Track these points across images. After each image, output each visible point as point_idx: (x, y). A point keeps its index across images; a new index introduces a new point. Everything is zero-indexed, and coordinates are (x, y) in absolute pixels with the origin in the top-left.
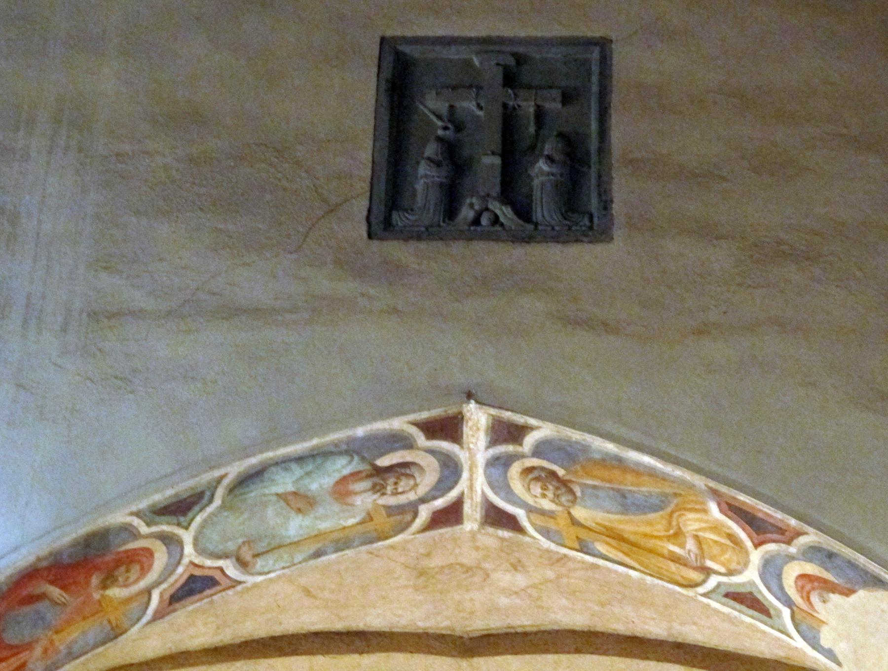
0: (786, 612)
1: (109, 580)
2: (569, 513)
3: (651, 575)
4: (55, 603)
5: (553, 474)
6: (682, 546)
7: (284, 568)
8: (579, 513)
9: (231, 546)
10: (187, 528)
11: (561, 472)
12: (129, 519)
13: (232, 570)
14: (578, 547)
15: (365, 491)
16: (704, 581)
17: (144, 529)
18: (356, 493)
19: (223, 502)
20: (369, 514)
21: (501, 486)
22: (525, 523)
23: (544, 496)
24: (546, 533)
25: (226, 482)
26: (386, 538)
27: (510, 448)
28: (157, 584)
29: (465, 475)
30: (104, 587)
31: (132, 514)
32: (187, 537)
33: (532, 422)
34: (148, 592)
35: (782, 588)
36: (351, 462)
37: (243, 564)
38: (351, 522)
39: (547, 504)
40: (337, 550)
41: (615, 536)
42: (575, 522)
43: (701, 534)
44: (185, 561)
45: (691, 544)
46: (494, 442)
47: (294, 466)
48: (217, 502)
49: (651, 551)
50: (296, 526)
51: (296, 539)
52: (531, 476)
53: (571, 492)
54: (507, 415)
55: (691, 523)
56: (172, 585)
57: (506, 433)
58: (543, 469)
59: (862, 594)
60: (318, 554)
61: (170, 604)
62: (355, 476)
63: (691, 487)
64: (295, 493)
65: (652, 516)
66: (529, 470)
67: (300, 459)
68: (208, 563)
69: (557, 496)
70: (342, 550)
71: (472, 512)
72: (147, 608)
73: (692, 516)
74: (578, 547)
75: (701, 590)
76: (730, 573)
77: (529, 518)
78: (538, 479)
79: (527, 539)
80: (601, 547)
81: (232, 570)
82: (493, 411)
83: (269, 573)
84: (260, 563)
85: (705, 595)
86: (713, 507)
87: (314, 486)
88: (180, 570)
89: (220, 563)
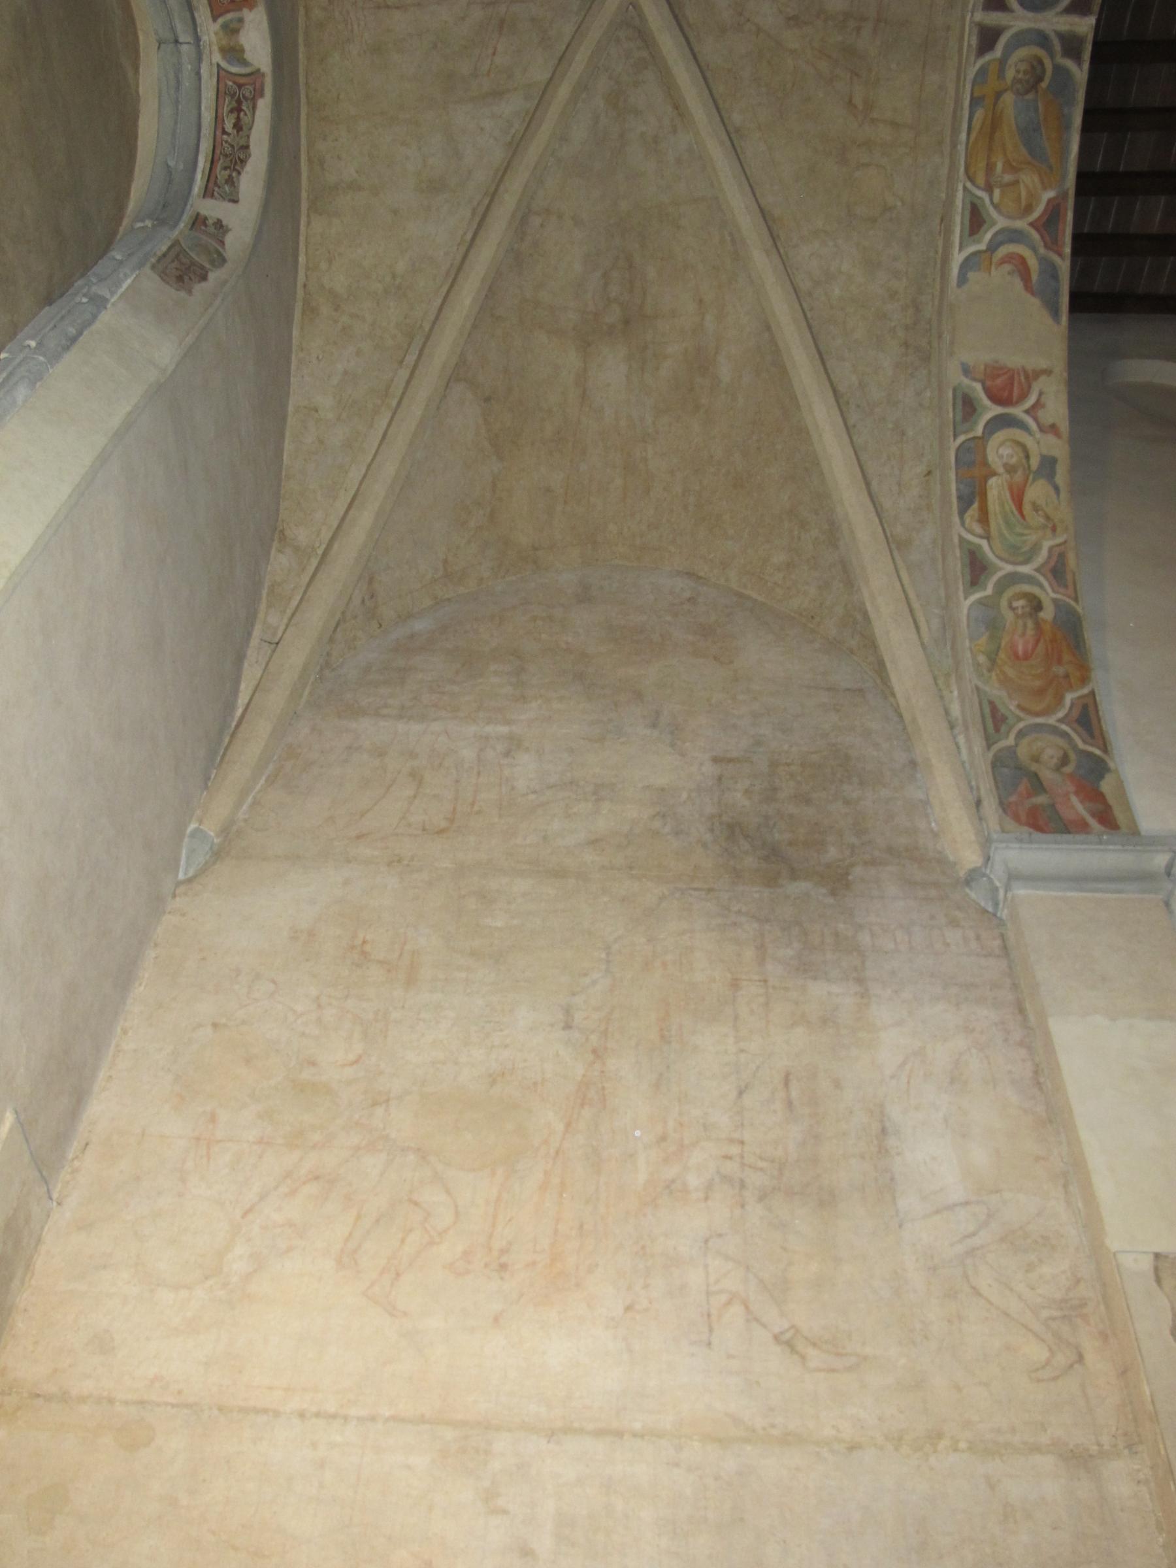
0: (982, 247)
2: (1006, 90)
3: (967, 149)
5: (1040, 79)
6: (1004, 171)
8: (1008, 98)
11: (1044, 85)
14: (976, 95)
16: (978, 187)
21: (1021, 39)
22: (988, 57)
23: (1018, 72)
24: (983, 72)
27: (1057, 47)
29: (1030, 15)
33: (1086, 66)
35: (1001, 243)
39: (1010, 74)
41: (994, 124)
42: (998, 95)
43: (1022, 185)
45: (1008, 178)
46: (1061, 36)
49: (990, 149)
52: (1035, 63)
53: (1027, 92)
54: (1088, 48)
55: (1029, 179)
57: (1071, 46)
58: (1044, 71)
59: (1035, 303)
63: (1064, 177)
65: (1024, 150)
66: (1041, 62)
69: (1020, 81)
71: (994, 18)
73: (1036, 179)
74: (976, 95)
75: (969, 185)
76: (996, 207)
77: (994, 60)
78: (1033, 67)
79: (973, 58)
80: (979, 114)
82: (1090, 38)
85: (965, 188)
86: (1051, 194)
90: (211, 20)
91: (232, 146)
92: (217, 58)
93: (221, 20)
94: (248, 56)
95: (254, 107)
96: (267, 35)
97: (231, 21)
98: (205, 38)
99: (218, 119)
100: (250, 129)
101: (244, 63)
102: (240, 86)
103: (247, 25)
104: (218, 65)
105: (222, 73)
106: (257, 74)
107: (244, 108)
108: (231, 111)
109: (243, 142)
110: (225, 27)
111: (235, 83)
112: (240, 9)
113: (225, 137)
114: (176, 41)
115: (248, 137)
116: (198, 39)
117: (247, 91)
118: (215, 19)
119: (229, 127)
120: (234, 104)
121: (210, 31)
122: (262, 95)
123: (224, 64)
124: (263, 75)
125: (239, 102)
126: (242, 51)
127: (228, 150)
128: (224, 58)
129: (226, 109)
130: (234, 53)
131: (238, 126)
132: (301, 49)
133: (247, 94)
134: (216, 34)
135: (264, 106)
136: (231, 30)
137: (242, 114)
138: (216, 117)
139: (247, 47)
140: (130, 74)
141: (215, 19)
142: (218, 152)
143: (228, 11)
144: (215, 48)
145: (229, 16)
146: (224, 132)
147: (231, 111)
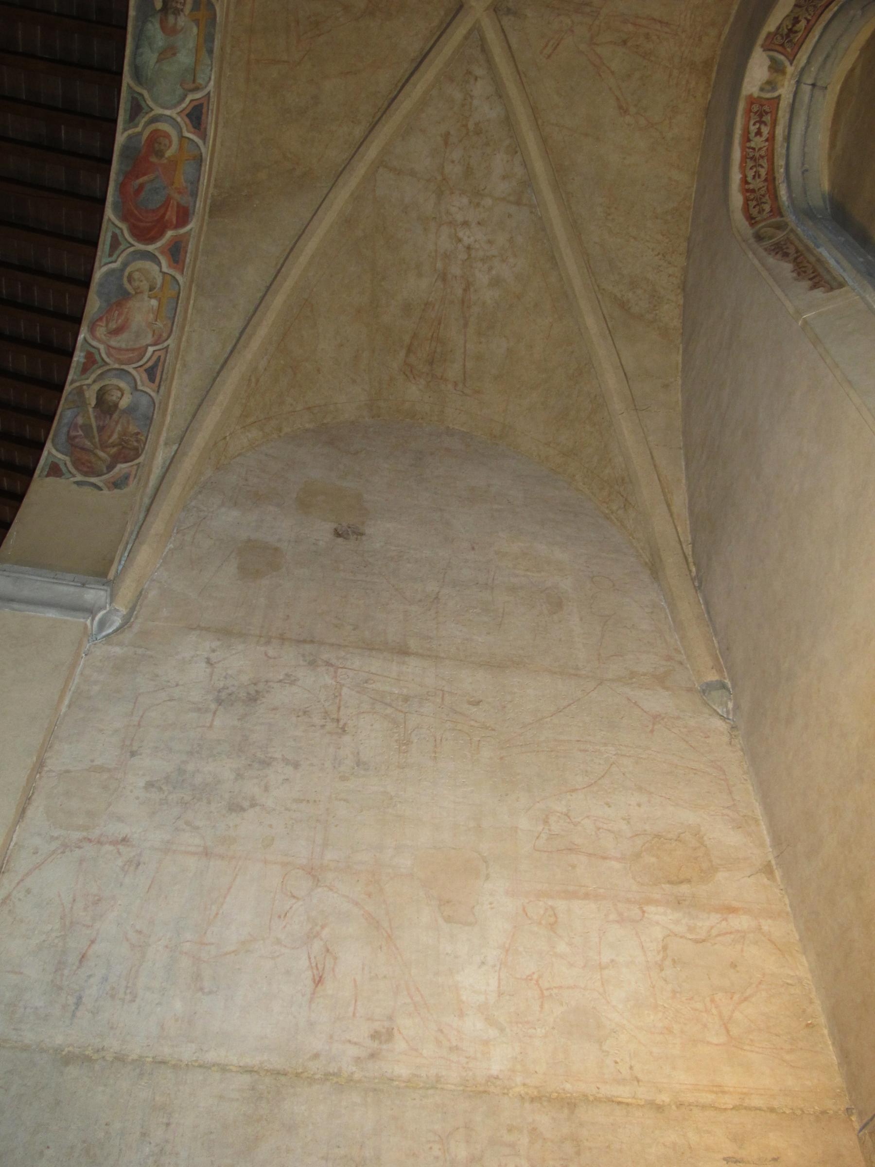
1: (160, 154)
4: (152, 181)
7: (211, 70)
9: (180, 91)
10: (152, 110)
12: (126, 134)
13: (198, 95)
15: (176, 19)
17: (139, 129)
18: (176, 24)
19: (146, 89)
20: (193, 21)
25: (132, 84)
26: (215, 15)
28: (180, 131)
30: (162, 156)
31: (123, 133)
32: (158, 111)
34: (182, 137)
36: (152, 22)
37: (197, 89)
38: (195, 30)
40: (213, 41)
44: (174, 116)
47: (141, 50)
48: (145, 93)
50: (184, 58)
51: (194, 59)
56: (187, 126)
60: (210, 52)
61: (199, 129)
62: (161, 22)
64: (160, 54)
67: (137, 47)
68: (184, 105)
70: (214, 39)
72: (193, 141)
81: (198, 95)
83: (210, 78)
84: (200, 81)
87: (160, 44)
88: (179, 119)
89: (187, 100)
90: (783, 96)
91: (807, 10)
92: (790, 69)
93: (776, 94)
94: (767, 63)
95: (778, 28)
96: (747, 74)
97: (769, 91)
98: (793, 82)
99: (809, 30)
100: (787, 16)
101: (772, 59)
102: (782, 45)
103: (760, 83)
104: (791, 64)
105: (791, 58)
106: (766, 48)
107: (786, 31)
108: (796, 32)
109: (798, 10)
110: (774, 89)
111: (785, 49)
112: (759, 98)
113: (809, 17)
114: (813, 85)
115: (792, 11)
116: (798, 82)
117: (779, 40)
118: (779, 97)
119: (803, 23)
120: (792, 36)
121: (785, 91)
122: (769, 34)
123: (787, 63)
124: (762, 46)
125: (788, 36)
126: (770, 67)
127: (811, 9)
128: (785, 67)
129: (800, 35)
130: (776, 68)
131: (796, 21)
132: (734, 12)
133: (779, 38)
134: (783, 86)
135: (772, 25)
136: (771, 85)
137: (790, 27)
138: (809, 32)
139: (765, 69)
140: (858, 71)
141: (779, 97)
142: (820, 11)
143: (768, 99)
144: (788, 76)
145: (769, 95)
146: (808, 21)
147: (796, 32)
